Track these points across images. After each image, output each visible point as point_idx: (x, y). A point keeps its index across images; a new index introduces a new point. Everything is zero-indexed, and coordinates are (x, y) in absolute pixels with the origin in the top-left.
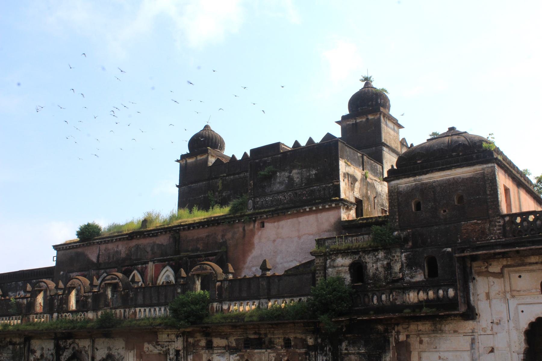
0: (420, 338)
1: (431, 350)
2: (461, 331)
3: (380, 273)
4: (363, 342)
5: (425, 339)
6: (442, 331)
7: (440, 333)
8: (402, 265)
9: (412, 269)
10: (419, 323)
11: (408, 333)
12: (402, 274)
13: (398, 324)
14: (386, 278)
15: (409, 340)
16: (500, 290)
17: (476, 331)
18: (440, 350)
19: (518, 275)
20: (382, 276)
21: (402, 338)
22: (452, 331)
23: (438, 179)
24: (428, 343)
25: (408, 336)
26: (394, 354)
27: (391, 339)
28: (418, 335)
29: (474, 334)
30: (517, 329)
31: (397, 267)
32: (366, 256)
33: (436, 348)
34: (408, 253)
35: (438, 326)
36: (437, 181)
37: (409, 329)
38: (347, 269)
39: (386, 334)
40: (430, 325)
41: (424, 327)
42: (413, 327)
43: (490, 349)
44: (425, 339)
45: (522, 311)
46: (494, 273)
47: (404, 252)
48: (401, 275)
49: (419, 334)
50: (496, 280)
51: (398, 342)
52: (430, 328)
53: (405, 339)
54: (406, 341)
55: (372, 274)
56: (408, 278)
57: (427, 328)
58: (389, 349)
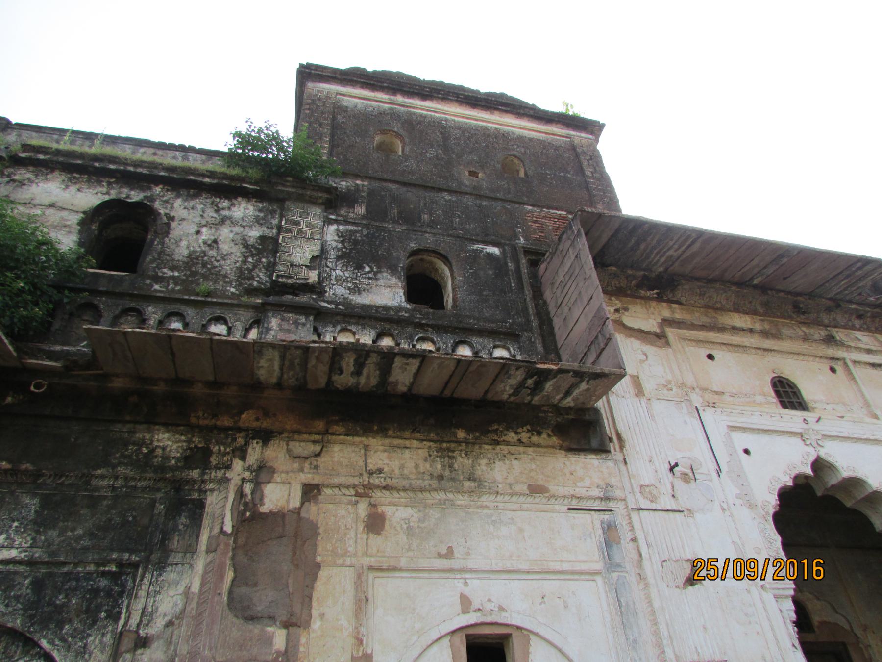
0: (373, 506)
1: (424, 563)
2: (561, 491)
3: (224, 257)
4: (31, 504)
5: (398, 512)
6: (478, 485)
7: (471, 492)
8: (323, 250)
9: (359, 267)
10: (375, 442)
11: (317, 480)
12: (319, 275)
13: (266, 437)
14: (243, 275)
15: (312, 511)
16: (670, 377)
17: (618, 493)
18: (471, 564)
19: (704, 352)
20: (228, 267)
21: (278, 496)
22: (523, 488)
23: (457, 119)
24: (410, 531)
25: (310, 492)
26: (213, 573)
27: (212, 501)
28: (364, 491)
29: (611, 505)
30: (751, 506)
31: (301, 253)
32: (178, 202)
33: (450, 553)
34: (350, 227)
35: (462, 462)
36: (454, 120)
37: (322, 461)
38: (74, 219)
39: (195, 474)
40: (423, 453)
41: (401, 458)
42: (345, 456)
43: (687, 570)
44: (398, 512)
45: (746, 451)
46: (640, 331)
47: (336, 221)
48: (313, 277)
49: (370, 487)
50: (650, 350)
51: (251, 518)
52: (425, 467)
53: (295, 503)
54: (298, 511)
55: (186, 252)
56: (340, 291)
57: (410, 465)
58: (191, 550)
